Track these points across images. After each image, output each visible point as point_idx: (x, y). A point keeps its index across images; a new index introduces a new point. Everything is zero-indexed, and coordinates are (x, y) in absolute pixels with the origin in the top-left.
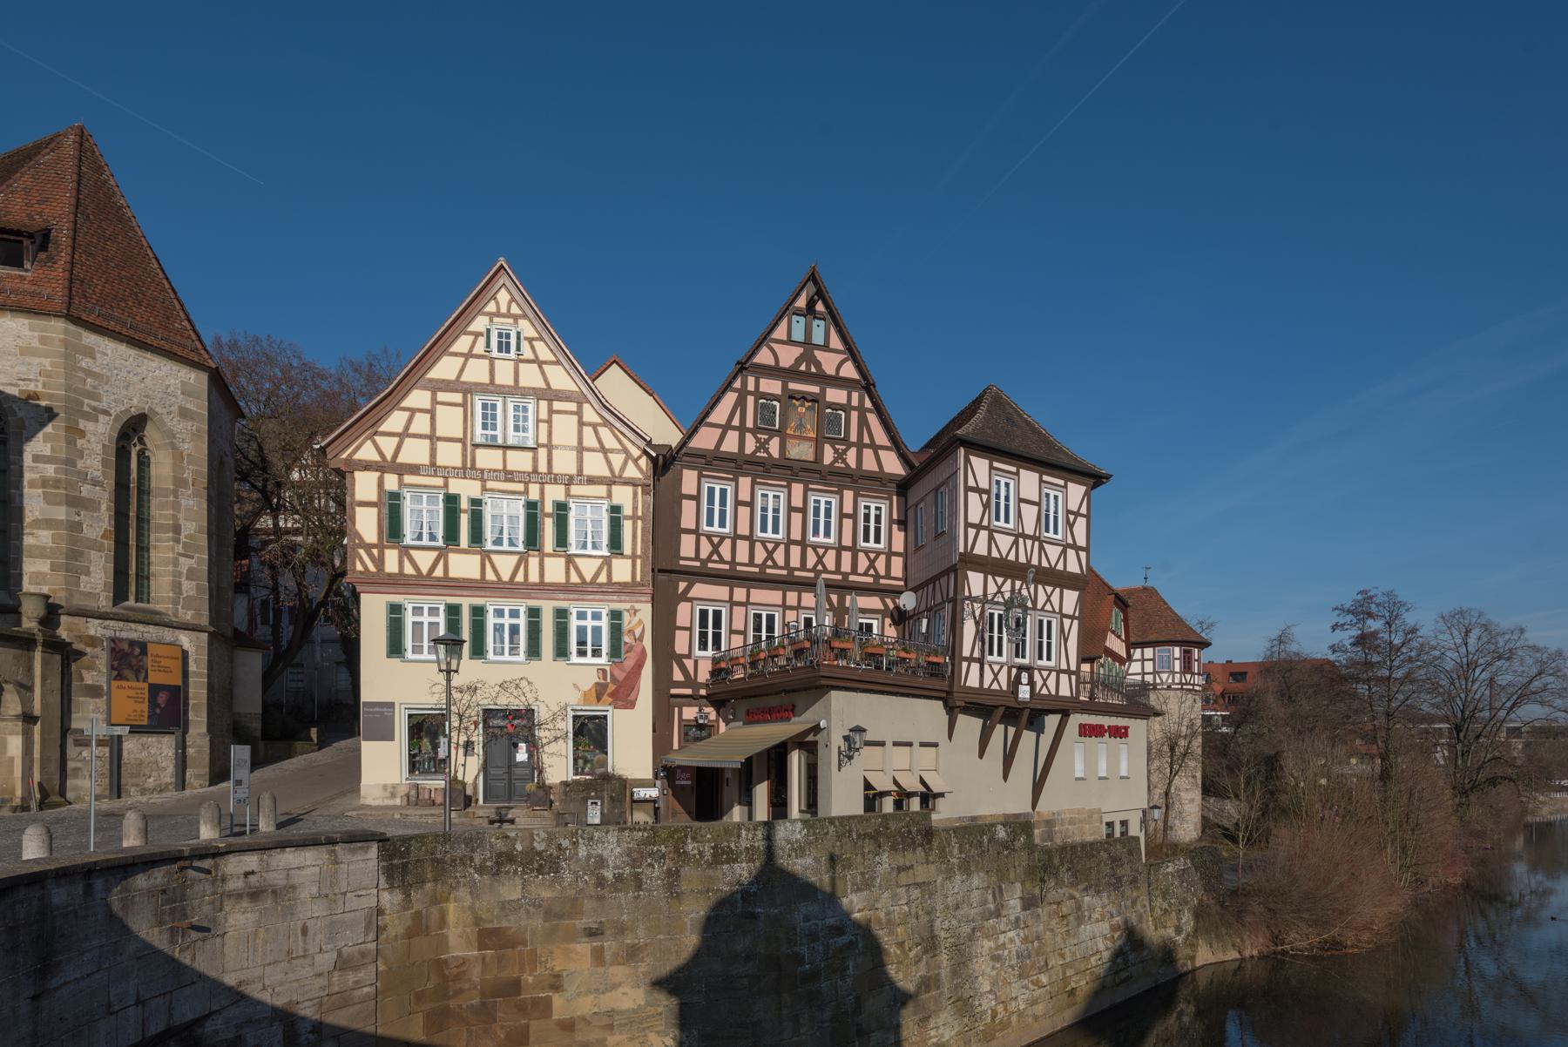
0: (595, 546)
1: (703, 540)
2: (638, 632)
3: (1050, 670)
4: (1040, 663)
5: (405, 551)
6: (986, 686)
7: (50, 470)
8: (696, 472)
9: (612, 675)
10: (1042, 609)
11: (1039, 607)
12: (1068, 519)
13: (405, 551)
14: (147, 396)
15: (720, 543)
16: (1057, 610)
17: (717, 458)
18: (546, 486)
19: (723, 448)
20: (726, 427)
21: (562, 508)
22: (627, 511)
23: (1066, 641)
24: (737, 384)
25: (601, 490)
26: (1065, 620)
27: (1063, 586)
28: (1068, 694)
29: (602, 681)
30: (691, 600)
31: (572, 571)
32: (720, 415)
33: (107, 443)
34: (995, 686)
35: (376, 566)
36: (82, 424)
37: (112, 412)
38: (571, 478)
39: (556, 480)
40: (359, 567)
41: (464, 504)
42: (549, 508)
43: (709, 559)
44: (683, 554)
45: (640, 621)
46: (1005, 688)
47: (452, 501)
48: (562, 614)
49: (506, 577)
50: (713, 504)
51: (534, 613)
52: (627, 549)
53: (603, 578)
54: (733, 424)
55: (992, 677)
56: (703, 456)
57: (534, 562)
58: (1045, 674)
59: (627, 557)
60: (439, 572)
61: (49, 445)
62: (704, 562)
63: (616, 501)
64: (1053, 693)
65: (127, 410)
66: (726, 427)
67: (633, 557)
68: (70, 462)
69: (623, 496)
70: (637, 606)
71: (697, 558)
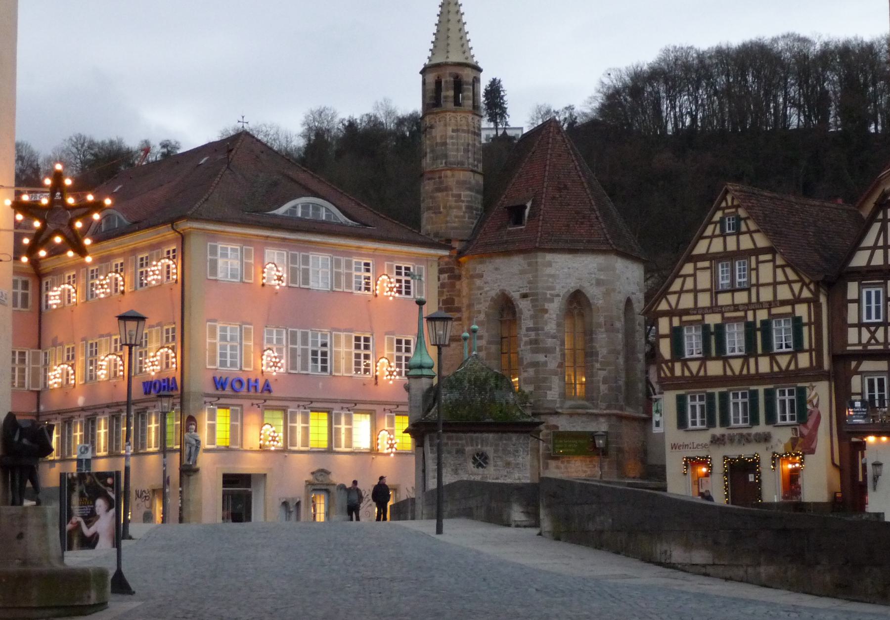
0: (787, 346)
1: (864, 330)
2: (815, 401)
5: (685, 363)
7: (533, 335)
8: (856, 283)
9: (800, 432)
13: (685, 363)
14: (579, 279)
15: (876, 330)
17: (869, 272)
18: (757, 311)
19: (873, 263)
20: (874, 248)
21: (766, 325)
22: (805, 320)
24: (881, 216)
25: (787, 309)
29: (795, 436)
30: (861, 373)
31: (774, 365)
32: (869, 240)
33: (558, 313)
35: (671, 373)
36: (547, 306)
37: (561, 294)
38: (770, 303)
39: (760, 305)
40: (663, 375)
41: (712, 329)
42: (758, 325)
43: (869, 343)
44: (850, 342)
45: (816, 394)
47: (706, 328)
48: (769, 394)
49: (737, 372)
50: (867, 307)
51: (754, 394)
52: (806, 345)
53: (792, 367)
54: (879, 245)
56: (859, 272)
57: (752, 361)
59: (806, 351)
60: (702, 373)
61: (532, 321)
62: (865, 346)
63: (798, 314)
65: (569, 290)
66: (874, 248)
67: (810, 351)
68: (543, 329)
69: (802, 310)
70: (814, 384)
71: (860, 343)
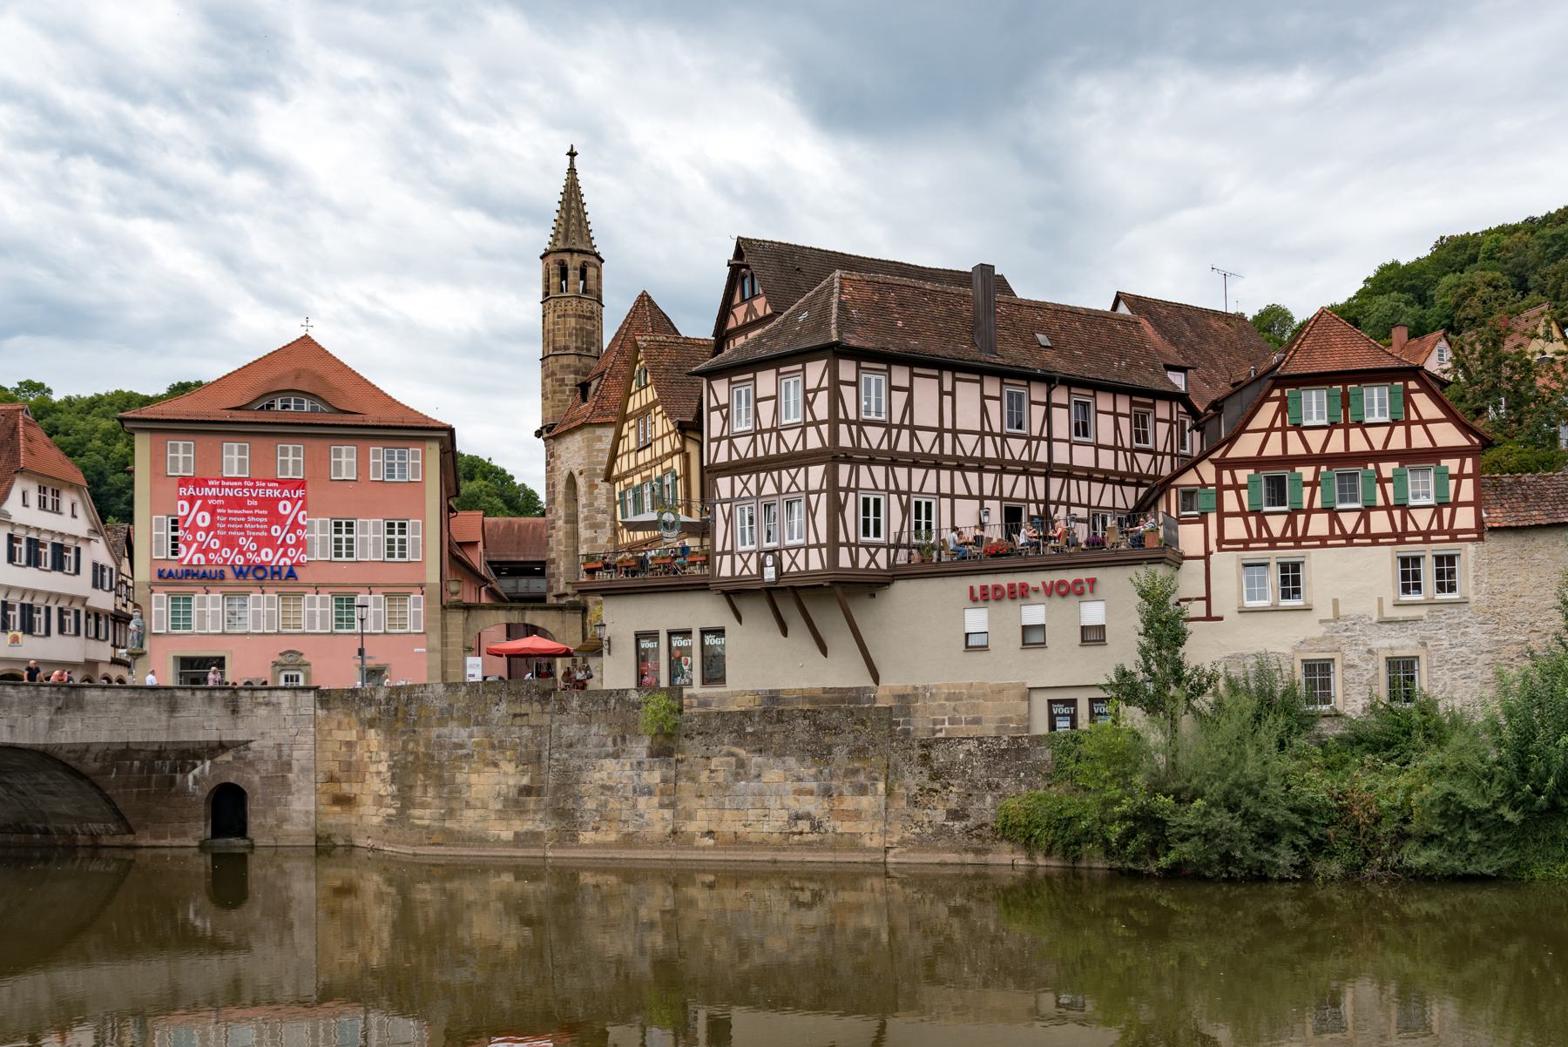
3: (798, 548)
4: (788, 543)
6: (737, 573)
10: (787, 492)
11: (784, 490)
12: (806, 398)
16: (803, 488)
23: (813, 516)
26: (811, 496)
27: (806, 465)
28: (820, 567)
34: (746, 572)
46: (754, 572)
55: (749, 564)
58: (793, 552)
64: (803, 568)
